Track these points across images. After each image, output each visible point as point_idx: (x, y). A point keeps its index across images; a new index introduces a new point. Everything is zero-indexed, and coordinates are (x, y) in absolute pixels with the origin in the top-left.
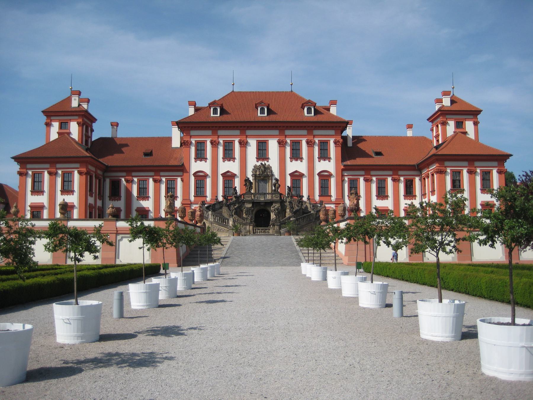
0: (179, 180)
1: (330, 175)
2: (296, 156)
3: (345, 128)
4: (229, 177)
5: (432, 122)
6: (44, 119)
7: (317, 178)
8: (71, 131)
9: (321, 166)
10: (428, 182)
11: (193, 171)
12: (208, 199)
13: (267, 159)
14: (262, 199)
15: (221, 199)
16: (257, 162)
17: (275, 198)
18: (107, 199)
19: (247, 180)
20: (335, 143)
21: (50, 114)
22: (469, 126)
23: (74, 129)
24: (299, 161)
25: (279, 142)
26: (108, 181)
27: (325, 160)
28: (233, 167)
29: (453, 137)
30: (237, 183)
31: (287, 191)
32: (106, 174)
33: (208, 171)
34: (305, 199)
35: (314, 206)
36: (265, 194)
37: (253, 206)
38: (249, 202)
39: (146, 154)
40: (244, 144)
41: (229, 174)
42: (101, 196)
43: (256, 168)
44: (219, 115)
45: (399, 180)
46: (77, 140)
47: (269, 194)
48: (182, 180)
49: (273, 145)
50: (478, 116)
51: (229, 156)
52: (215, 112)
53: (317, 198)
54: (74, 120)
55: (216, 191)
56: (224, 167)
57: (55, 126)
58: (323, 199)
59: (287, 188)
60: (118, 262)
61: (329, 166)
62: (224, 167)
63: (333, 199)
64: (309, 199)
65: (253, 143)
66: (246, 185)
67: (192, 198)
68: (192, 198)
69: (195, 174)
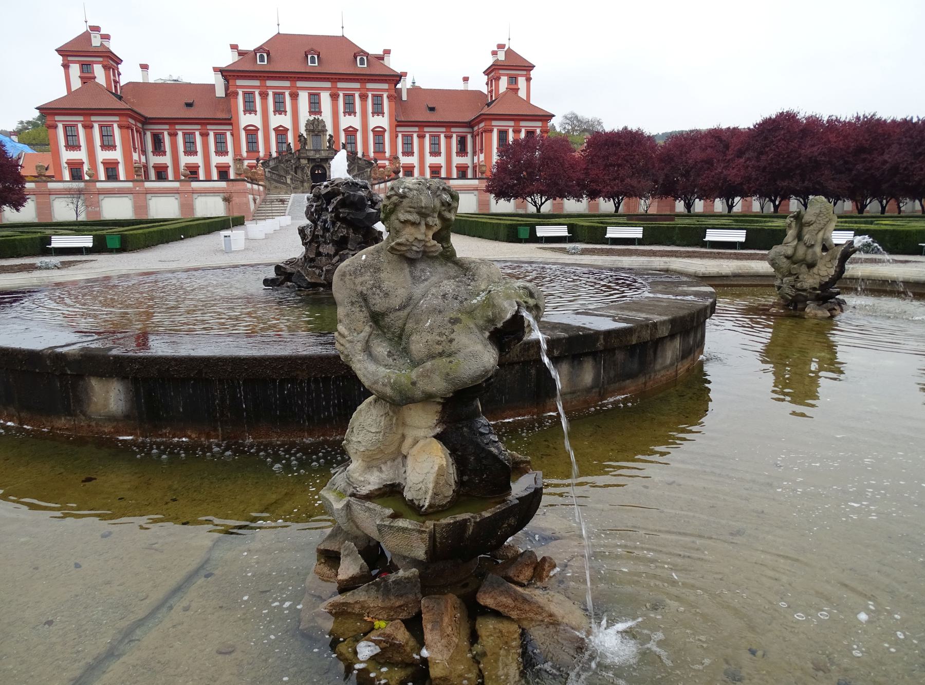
0: (228, 134)
1: (385, 130)
2: (350, 111)
3: (398, 82)
4: (281, 132)
5: (487, 75)
6: (60, 59)
7: (371, 135)
8: (96, 74)
9: (375, 121)
10: (478, 139)
11: (243, 125)
12: (262, 154)
13: (320, 113)
15: (274, 155)
18: (150, 154)
19: (301, 136)
21: (67, 53)
22: (522, 82)
23: (99, 72)
26: (149, 134)
28: (285, 120)
29: (505, 94)
30: (290, 138)
34: (360, 155)
35: (369, 164)
38: (304, 158)
39: (189, 105)
40: (294, 96)
42: (144, 152)
43: (309, 123)
45: (451, 137)
48: (232, 135)
49: (325, 98)
50: (532, 72)
51: (280, 109)
52: (262, 60)
53: (372, 155)
55: (268, 146)
56: (276, 120)
57: (75, 69)
58: (378, 155)
61: (383, 121)
62: (276, 120)
63: (387, 155)
64: (363, 155)
65: (304, 97)
66: (300, 141)
67: (245, 154)
68: (245, 154)
69: (245, 129)
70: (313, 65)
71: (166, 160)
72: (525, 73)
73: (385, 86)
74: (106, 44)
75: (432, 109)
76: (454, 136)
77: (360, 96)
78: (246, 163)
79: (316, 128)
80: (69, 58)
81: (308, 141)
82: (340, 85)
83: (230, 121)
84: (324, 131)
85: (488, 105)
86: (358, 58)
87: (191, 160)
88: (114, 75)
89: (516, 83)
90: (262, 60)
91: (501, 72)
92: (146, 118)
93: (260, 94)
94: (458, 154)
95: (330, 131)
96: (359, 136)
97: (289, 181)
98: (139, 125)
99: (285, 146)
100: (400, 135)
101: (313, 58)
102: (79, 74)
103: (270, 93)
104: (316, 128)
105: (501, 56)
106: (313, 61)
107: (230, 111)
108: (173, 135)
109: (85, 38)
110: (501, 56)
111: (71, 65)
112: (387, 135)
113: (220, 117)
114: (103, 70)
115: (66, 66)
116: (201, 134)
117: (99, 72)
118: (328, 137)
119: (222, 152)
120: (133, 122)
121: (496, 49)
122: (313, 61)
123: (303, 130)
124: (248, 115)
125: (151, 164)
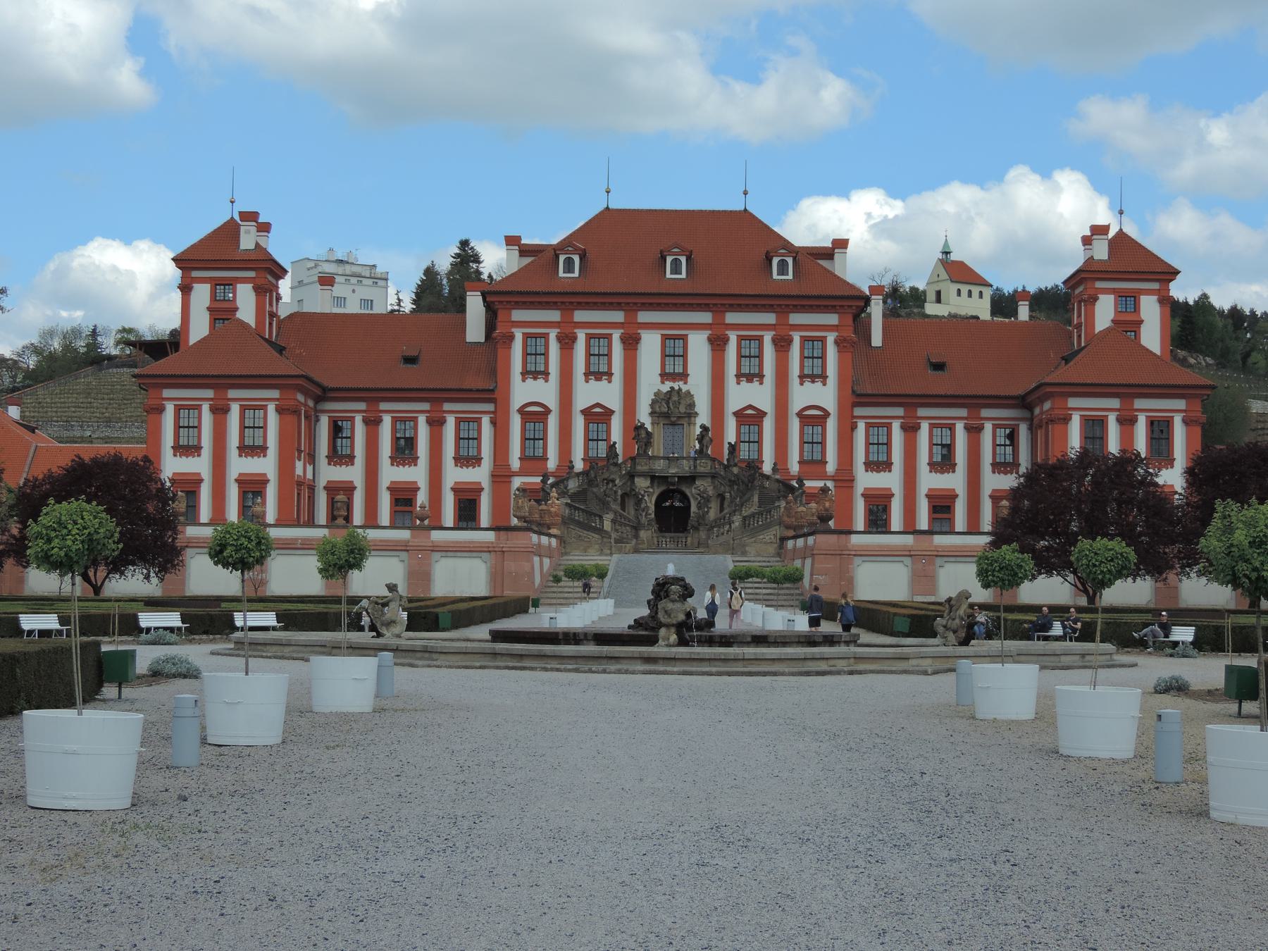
0: (486, 421)
1: (827, 414)
4: (598, 416)
7: (795, 425)
8: (239, 303)
12: (552, 464)
13: (684, 376)
14: (673, 471)
15: (579, 466)
16: (663, 383)
17: (702, 469)
20: (836, 342)
24: (756, 384)
25: (709, 339)
26: (324, 422)
27: (813, 382)
28: (609, 394)
29: (1108, 330)
30: (616, 434)
31: (726, 452)
32: (320, 407)
33: (552, 401)
34: (767, 468)
35: (786, 488)
36: (677, 459)
37: (652, 486)
39: (410, 360)
40: (631, 343)
41: (598, 410)
44: (576, 274)
45: (980, 429)
46: (253, 325)
47: (688, 458)
48: (493, 422)
52: (569, 265)
53: (794, 468)
54: (244, 280)
57: (202, 294)
59: (726, 446)
60: (433, 595)
62: (587, 393)
63: (831, 468)
64: (775, 470)
65: (651, 343)
67: (515, 464)
68: (515, 464)
70: (676, 274)
71: (354, 474)
72: (1156, 286)
73: (832, 319)
74: (263, 244)
75: (939, 367)
76: (988, 427)
77: (775, 341)
78: (517, 482)
79: (673, 409)
80: (195, 274)
81: (656, 436)
82: (731, 318)
83: (491, 393)
84: (691, 415)
85: (1067, 360)
86: (775, 261)
87: (404, 474)
88: (271, 304)
89: (1137, 309)
90: (569, 265)
91: (1099, 285)
92: (325, 389)
93: (560, 339)
94: (933, 466)
95: (704, 416)
96: (768, 425)
97: (607, 525)
98: (311, 403)
99: (603, 446)
100: (861, 426)
101: (676, 263)
102: (208, 304)
103: (581, 336)
104: (673, 409)
105: (1101, 251)
106: (676, 270)
107: (493, 372)
108: (373, 423)
109: (229, 232)
110: (1101, 251)
111: (196, 286)
112: (832, 425)
113: (473, 386)
114: (253, 294)
115: (185, 289)
116: (430, 422)
117: (246, 303)
118: (698, 431)
119: (464, 460)
120: (301, 398)
121: (1089, 233)
122: (676, 270)
123: (644, 416)
124: (530, 381)
125: (322, 482)
